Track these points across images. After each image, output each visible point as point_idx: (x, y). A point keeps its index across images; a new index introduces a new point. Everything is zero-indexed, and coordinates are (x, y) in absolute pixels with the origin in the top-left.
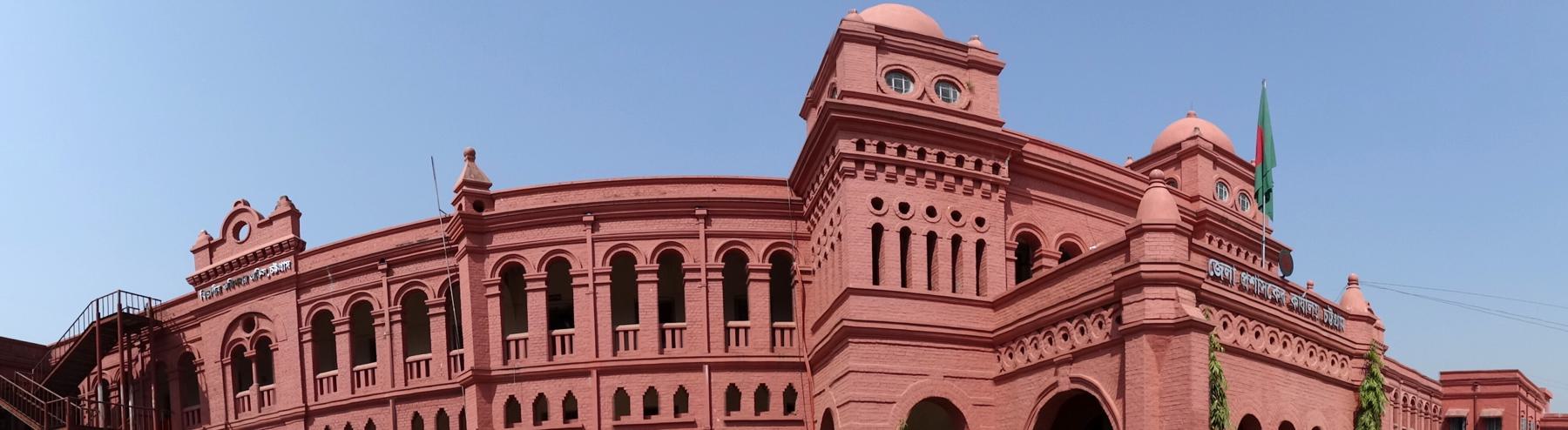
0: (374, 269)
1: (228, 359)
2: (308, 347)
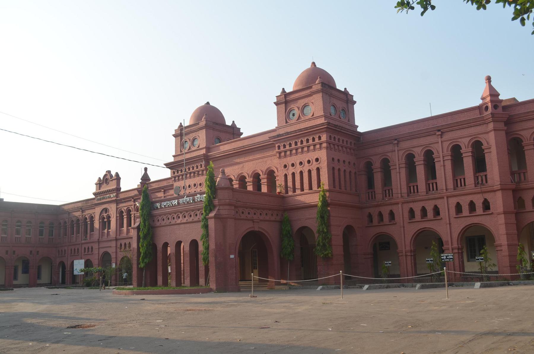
0: (131, 200)
1: (101, 220)
2: (118, 220)
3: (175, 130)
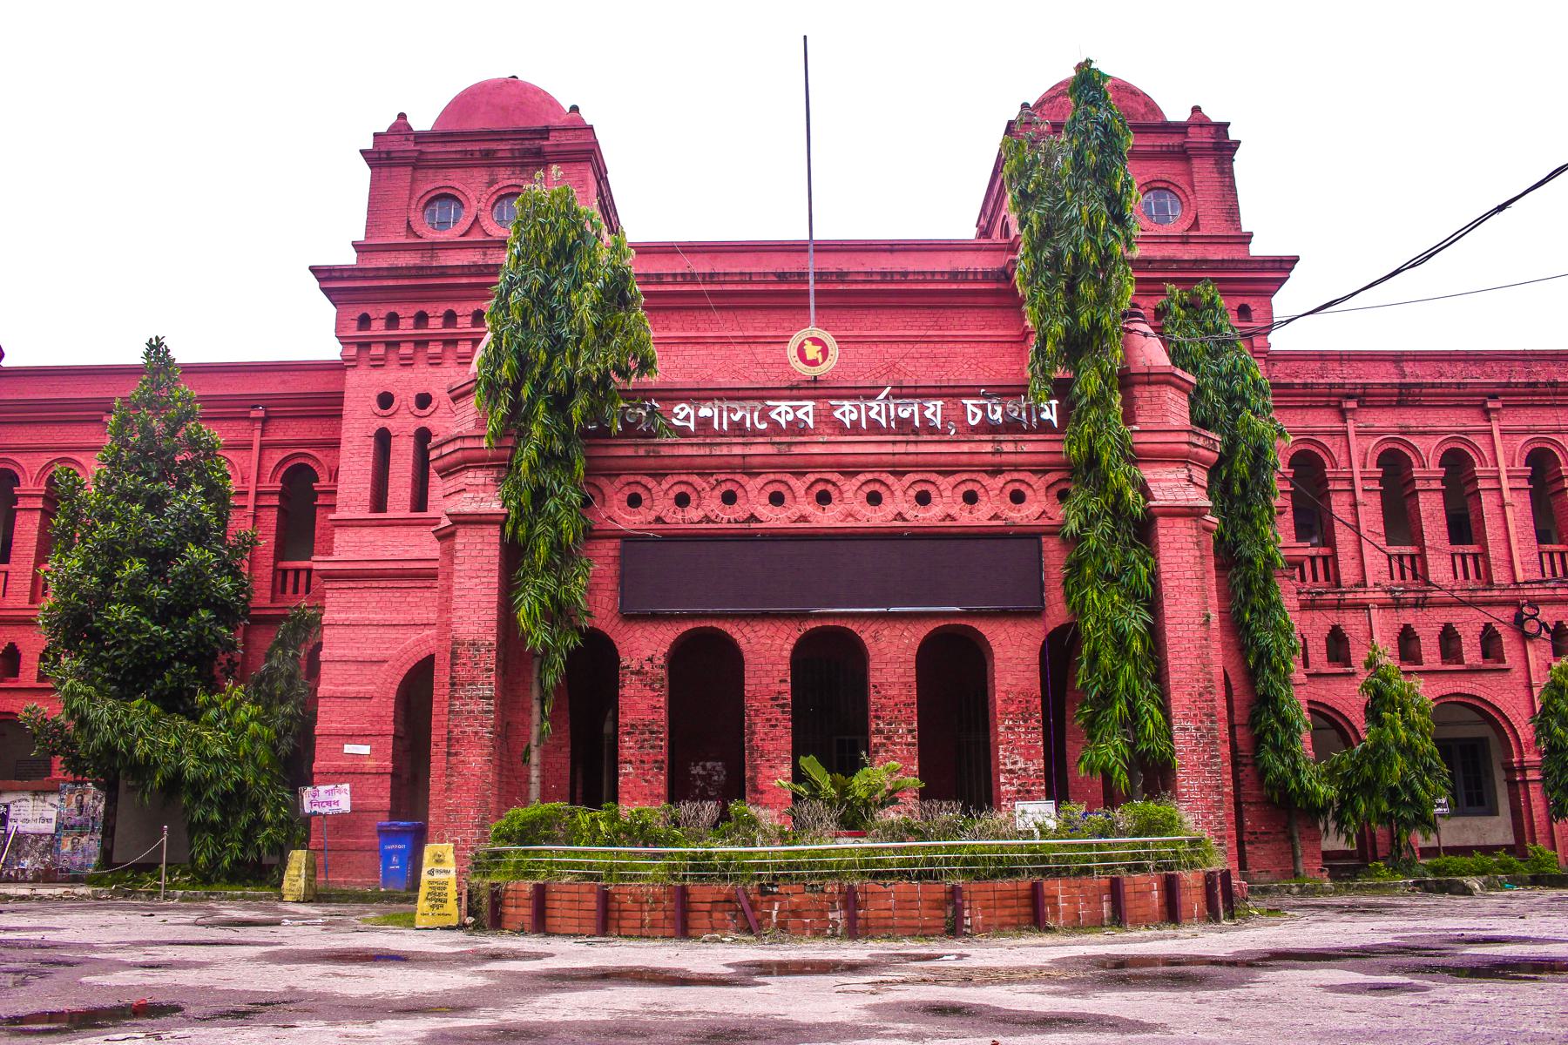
3: (375, 135)
